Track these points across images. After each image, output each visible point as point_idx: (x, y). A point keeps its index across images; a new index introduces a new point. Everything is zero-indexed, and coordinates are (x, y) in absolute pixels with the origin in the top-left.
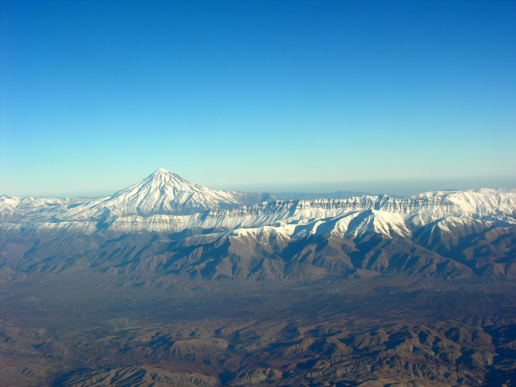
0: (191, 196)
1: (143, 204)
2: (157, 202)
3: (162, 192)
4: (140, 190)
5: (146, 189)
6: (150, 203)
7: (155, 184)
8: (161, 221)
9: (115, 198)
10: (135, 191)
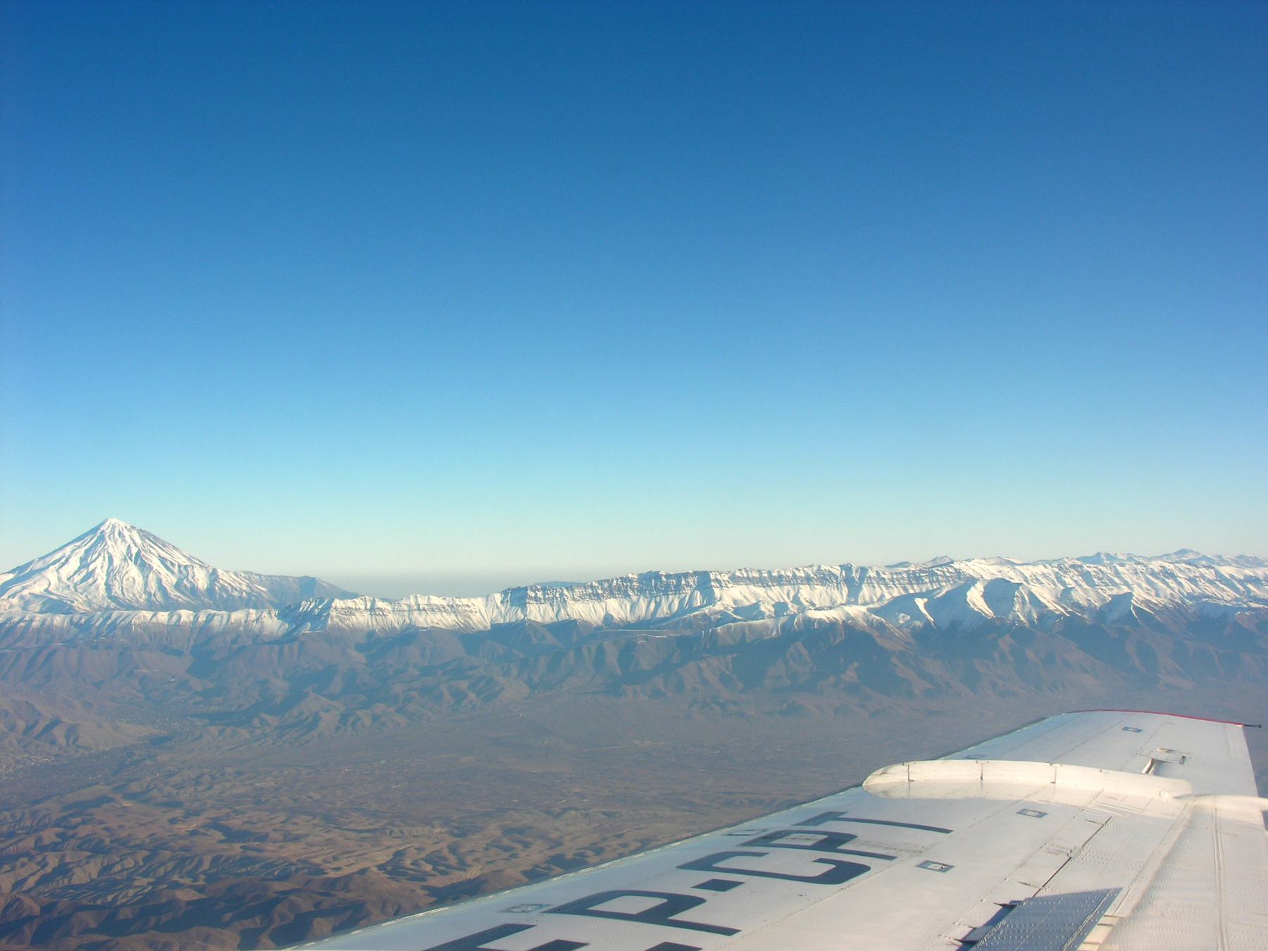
0: (214, 576)
1: (116, 590)
2: (146, 585)
3: (144, 567)
4: (84, 563)
5: (101, 559)
6: (132, 587)
7: (117, 550)
8: (433, 609)
9: (37, 577)
10: (74, 563)
